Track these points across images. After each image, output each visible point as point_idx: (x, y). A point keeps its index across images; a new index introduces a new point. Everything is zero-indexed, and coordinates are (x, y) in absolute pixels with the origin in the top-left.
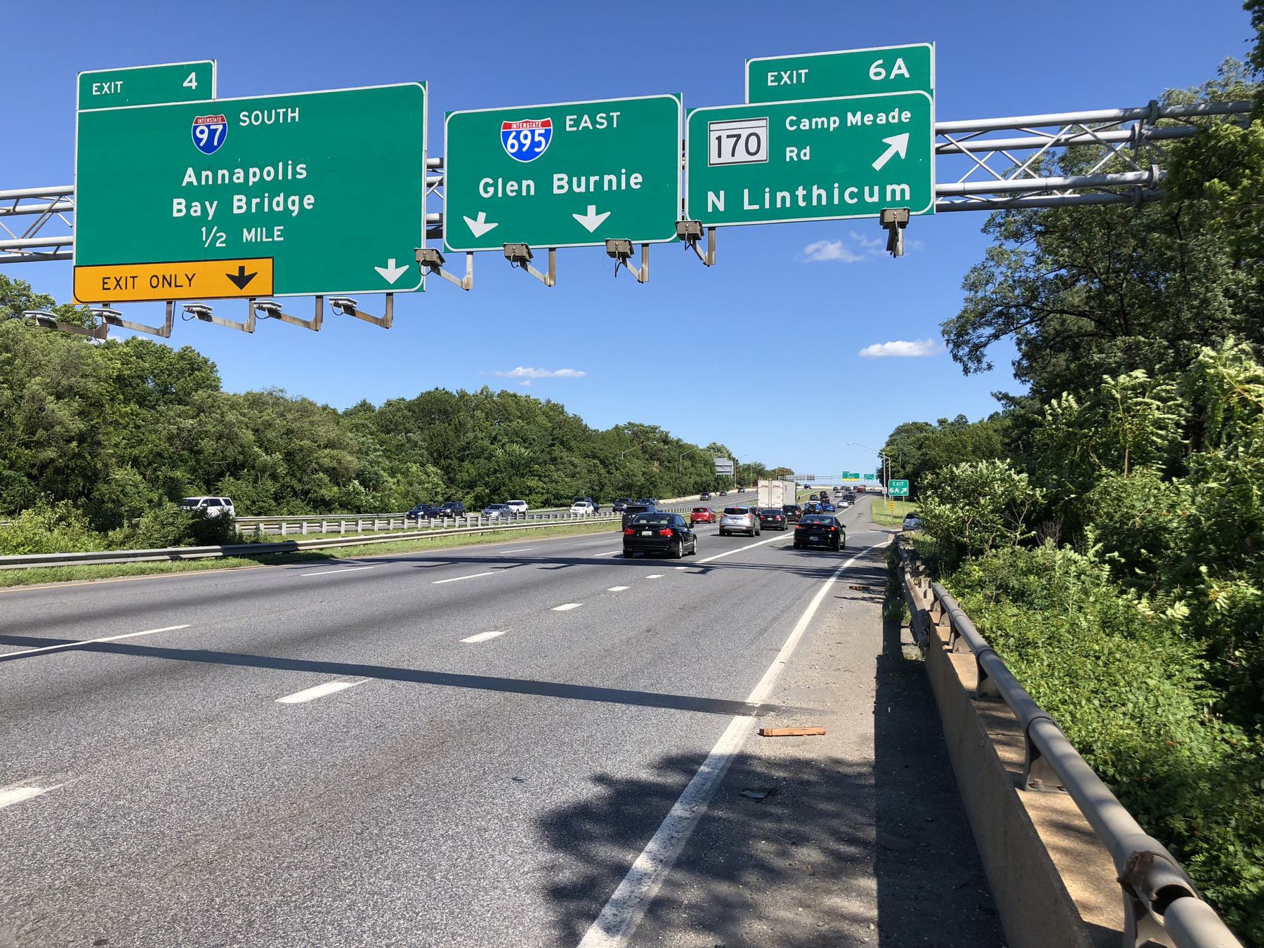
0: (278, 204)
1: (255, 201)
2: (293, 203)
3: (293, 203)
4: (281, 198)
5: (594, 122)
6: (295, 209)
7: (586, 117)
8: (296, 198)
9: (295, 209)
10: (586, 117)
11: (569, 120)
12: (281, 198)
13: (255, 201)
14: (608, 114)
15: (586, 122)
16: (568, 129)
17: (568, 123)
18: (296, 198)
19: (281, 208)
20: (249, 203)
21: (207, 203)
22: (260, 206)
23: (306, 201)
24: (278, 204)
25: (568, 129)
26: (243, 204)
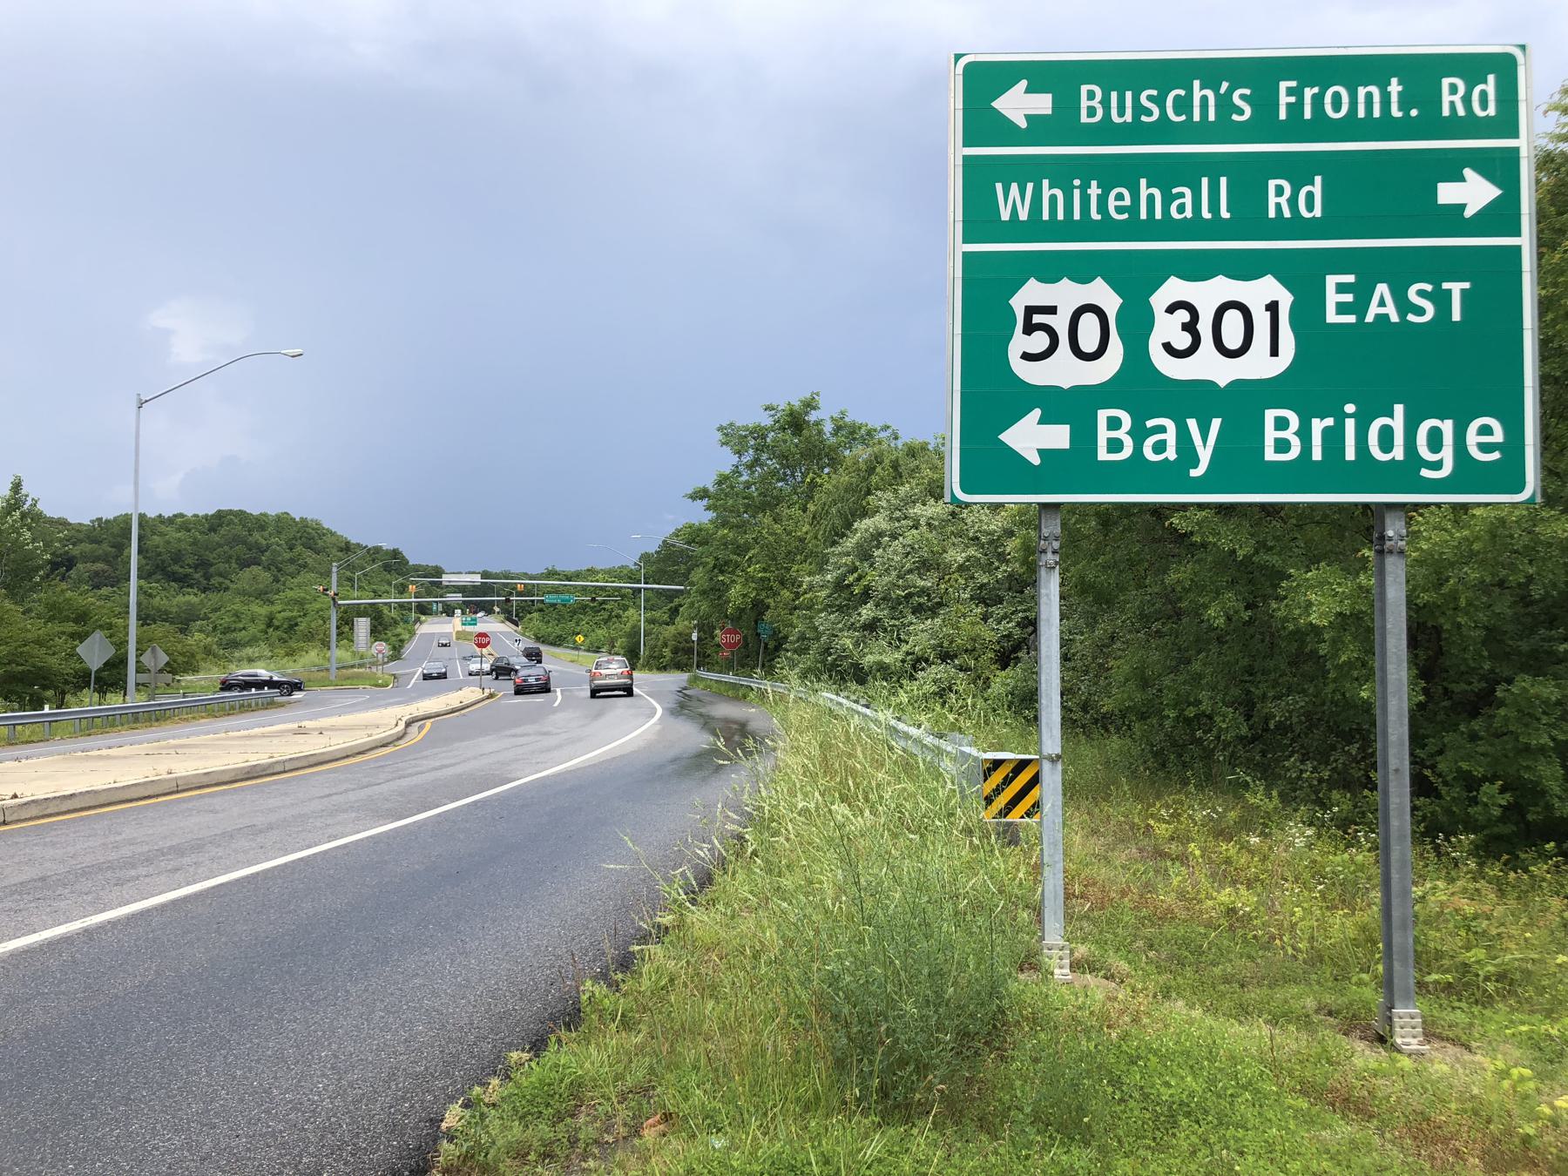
0: (1386, 436)
1: (1318, 426)
5: (1404, 306)
7: (1382, 289)
10: (1382, 289)
11: (1334, 292)
12: (1398, 422)
14: (1437, 286)
15: (1382, 303)
16: (1332, 317)
17: (1332, 298)
20: (1304, 433)
21: (1192, 424)
22: (1333, 438)
24: (1386, 436)
25: (1332, 317)
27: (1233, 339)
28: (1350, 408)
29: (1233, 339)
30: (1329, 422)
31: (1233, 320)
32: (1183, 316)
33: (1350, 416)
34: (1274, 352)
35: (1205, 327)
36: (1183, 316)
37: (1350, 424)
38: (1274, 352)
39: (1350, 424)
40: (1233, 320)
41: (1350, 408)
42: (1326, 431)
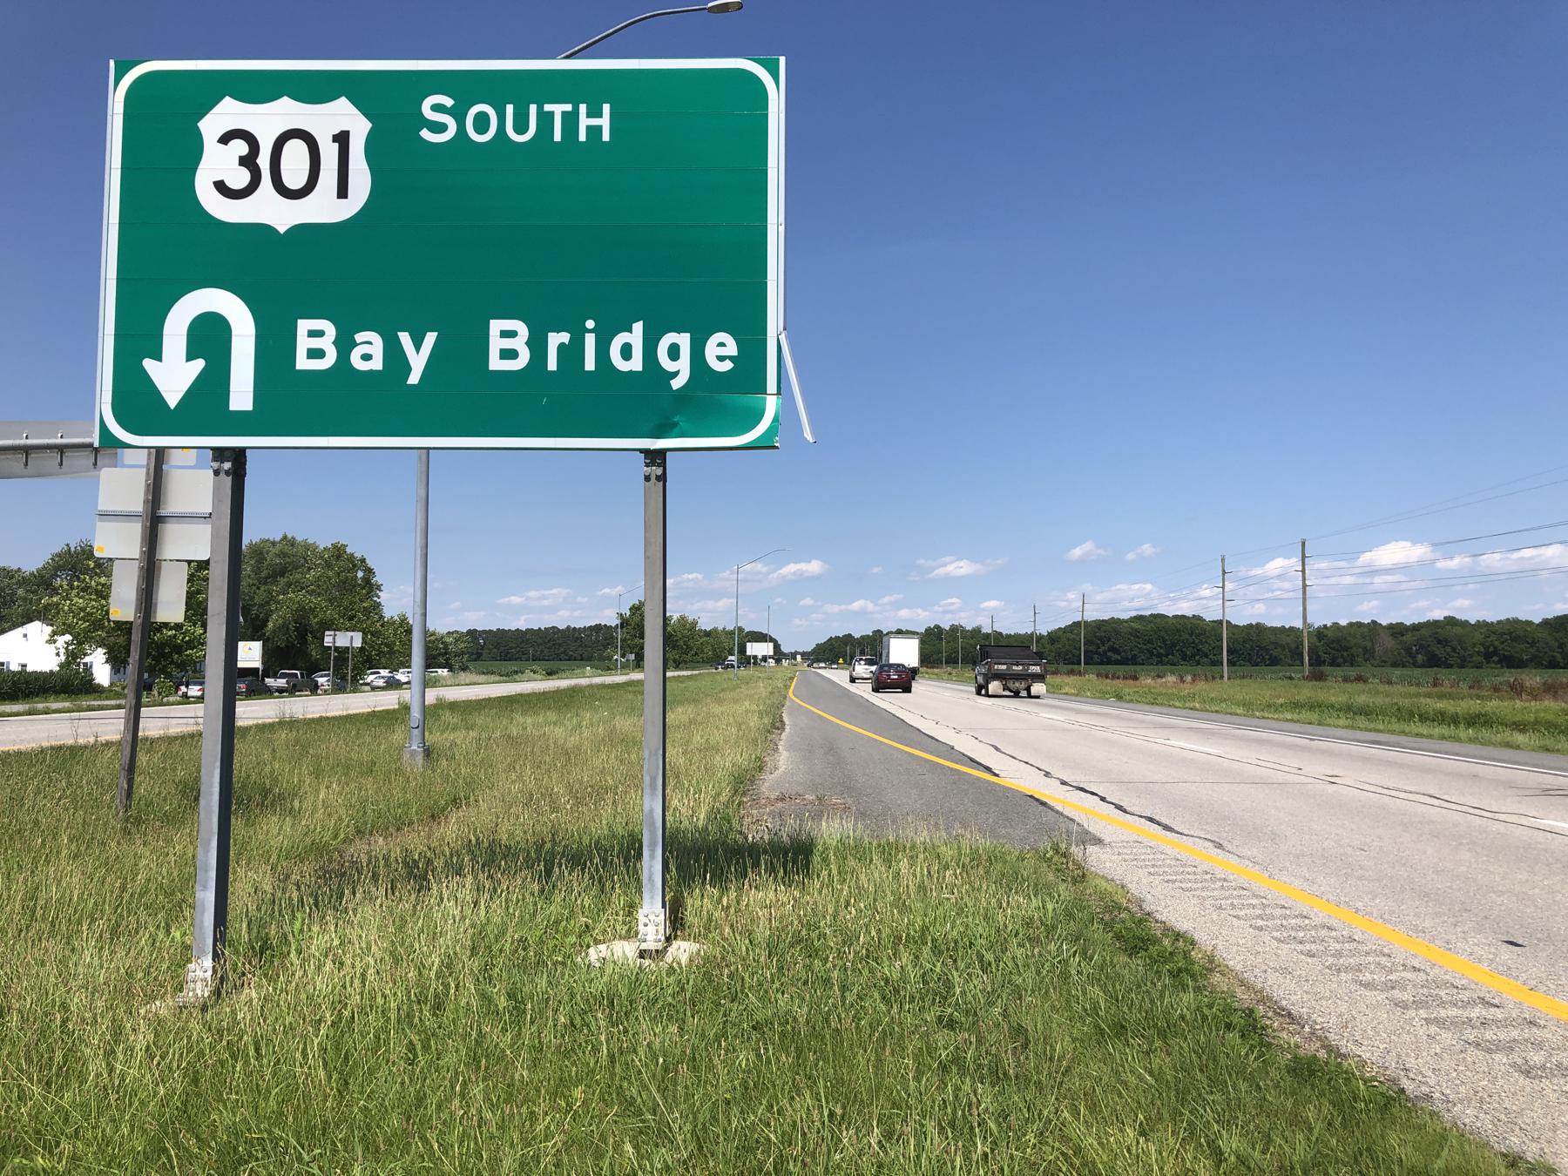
0: (626, 352)
2: (674, 352)
3: (674, 352)
4: (635, 336)
6: (681, 372)
8: (684, 340)
9: (681, 372)
12: (635, 336)
13: (556, 339)
18: (684, 340)
19: (636, 364)
20: (537, 345)
22: (571, 354)
23: (711, 351)
24: (626, 352)
26: (520, 344)
27: (295, 176)
28: (590, 324)
29: (295, 176)
30: (565, 337)
31: (296, 152)
32: (241, 147)
33: (590, 331)
34: (343, 192)
35: (264, 161)
36: (241, 147)
37: (590, 340)
38: (343, 192)
39: (590, 340)
40: (296, 152)
41: (590, 324)
42: (561, 347)
